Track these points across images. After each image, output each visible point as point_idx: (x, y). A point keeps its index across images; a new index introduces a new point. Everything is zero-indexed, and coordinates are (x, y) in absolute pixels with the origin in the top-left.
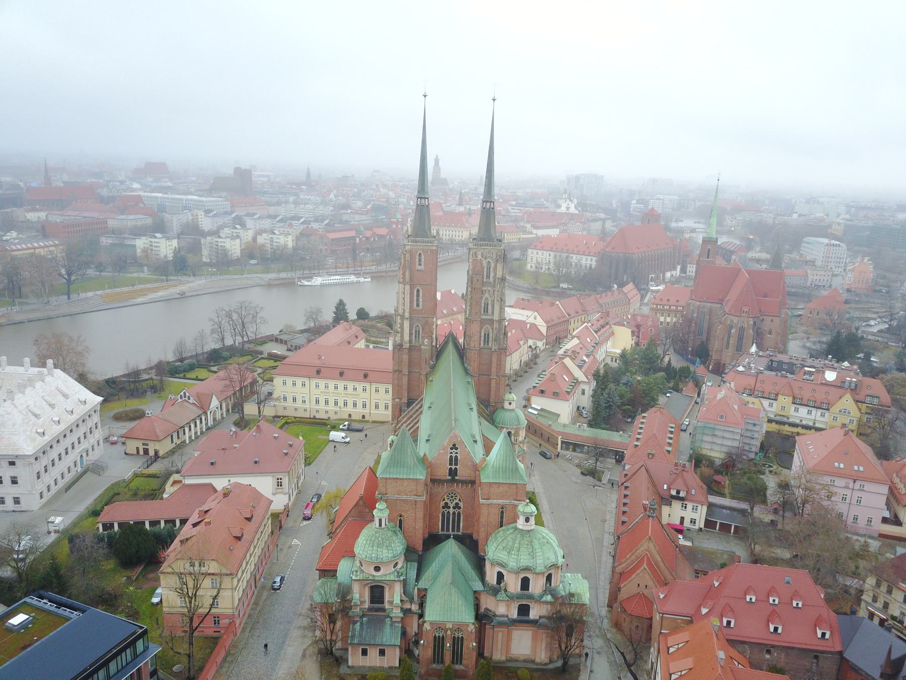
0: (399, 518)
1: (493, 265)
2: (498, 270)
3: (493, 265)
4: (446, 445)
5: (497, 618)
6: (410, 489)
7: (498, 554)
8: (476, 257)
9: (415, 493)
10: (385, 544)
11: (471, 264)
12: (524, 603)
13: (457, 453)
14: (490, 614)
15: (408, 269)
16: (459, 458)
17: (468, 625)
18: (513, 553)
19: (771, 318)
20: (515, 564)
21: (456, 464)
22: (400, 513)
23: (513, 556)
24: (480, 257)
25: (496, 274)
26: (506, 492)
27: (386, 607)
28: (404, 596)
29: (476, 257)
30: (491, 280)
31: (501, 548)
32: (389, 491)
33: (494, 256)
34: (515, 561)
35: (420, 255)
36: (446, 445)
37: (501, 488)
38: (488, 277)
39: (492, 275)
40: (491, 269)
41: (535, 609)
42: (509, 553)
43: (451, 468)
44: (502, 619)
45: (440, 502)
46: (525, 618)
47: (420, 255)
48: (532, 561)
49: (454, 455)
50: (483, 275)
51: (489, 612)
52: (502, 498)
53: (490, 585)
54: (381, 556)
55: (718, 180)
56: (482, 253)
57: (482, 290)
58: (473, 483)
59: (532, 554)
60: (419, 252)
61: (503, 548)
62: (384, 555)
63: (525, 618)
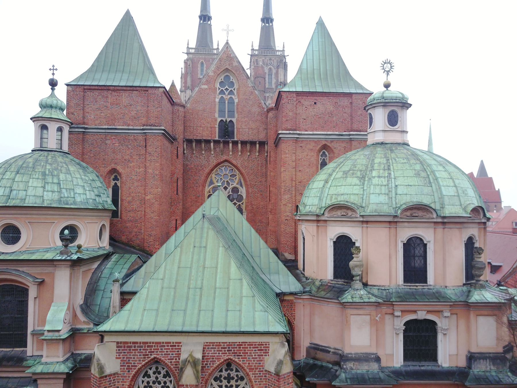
0: (113, 183)
1: (274, 71)
2: (279, 75)
3: (274, 71)
4: (211, 74)
5: (349, 365)
6: (133, 113)
7: (333, 191)
8: (257, 64)
9: (144, 121)
10: (39, 169)
11: (253, 71)
12: (421, 315)
13: (231, 92)
14: (325, 360)
15: (189, 74)
16: (236, 101)
17: (264, 349)
18: (374, 173)
19: (494, 204)
20: (383, 199)
22: (113, 166)
23: (375, 181)
24: (261, 63)
25: (277, 80)
26: (331, 114)
27: (29, 353)
28: (82, 317)
29: (257, 64)
30: (274, 86)
31: (340, 175)
32: (90, 116)
33: (275, 64)
34: (384, 190)
35: (202, 63)
36: (211, 74)
37: (319, 105)
38: (270, 83)
39: (274, 81)
40: (273, 76)
42: (362, 178)
44: (363, 369)
45: (204, 186)
46: (427, 366)
47: (202, 63)
48: (427, 190)
49: (226, 97)
50: (265, 78)
51: (320, 355)
52: (322, 128)
53: (318, 283)
54: (22, 194)
55: (430, 120)
56: (263, 60)
57: (265, 97)
58: (262, 144)
59: (423, 174)
60: (201, 61)
61: (345, 173)
62: (30, 192)
63: (427, 366)
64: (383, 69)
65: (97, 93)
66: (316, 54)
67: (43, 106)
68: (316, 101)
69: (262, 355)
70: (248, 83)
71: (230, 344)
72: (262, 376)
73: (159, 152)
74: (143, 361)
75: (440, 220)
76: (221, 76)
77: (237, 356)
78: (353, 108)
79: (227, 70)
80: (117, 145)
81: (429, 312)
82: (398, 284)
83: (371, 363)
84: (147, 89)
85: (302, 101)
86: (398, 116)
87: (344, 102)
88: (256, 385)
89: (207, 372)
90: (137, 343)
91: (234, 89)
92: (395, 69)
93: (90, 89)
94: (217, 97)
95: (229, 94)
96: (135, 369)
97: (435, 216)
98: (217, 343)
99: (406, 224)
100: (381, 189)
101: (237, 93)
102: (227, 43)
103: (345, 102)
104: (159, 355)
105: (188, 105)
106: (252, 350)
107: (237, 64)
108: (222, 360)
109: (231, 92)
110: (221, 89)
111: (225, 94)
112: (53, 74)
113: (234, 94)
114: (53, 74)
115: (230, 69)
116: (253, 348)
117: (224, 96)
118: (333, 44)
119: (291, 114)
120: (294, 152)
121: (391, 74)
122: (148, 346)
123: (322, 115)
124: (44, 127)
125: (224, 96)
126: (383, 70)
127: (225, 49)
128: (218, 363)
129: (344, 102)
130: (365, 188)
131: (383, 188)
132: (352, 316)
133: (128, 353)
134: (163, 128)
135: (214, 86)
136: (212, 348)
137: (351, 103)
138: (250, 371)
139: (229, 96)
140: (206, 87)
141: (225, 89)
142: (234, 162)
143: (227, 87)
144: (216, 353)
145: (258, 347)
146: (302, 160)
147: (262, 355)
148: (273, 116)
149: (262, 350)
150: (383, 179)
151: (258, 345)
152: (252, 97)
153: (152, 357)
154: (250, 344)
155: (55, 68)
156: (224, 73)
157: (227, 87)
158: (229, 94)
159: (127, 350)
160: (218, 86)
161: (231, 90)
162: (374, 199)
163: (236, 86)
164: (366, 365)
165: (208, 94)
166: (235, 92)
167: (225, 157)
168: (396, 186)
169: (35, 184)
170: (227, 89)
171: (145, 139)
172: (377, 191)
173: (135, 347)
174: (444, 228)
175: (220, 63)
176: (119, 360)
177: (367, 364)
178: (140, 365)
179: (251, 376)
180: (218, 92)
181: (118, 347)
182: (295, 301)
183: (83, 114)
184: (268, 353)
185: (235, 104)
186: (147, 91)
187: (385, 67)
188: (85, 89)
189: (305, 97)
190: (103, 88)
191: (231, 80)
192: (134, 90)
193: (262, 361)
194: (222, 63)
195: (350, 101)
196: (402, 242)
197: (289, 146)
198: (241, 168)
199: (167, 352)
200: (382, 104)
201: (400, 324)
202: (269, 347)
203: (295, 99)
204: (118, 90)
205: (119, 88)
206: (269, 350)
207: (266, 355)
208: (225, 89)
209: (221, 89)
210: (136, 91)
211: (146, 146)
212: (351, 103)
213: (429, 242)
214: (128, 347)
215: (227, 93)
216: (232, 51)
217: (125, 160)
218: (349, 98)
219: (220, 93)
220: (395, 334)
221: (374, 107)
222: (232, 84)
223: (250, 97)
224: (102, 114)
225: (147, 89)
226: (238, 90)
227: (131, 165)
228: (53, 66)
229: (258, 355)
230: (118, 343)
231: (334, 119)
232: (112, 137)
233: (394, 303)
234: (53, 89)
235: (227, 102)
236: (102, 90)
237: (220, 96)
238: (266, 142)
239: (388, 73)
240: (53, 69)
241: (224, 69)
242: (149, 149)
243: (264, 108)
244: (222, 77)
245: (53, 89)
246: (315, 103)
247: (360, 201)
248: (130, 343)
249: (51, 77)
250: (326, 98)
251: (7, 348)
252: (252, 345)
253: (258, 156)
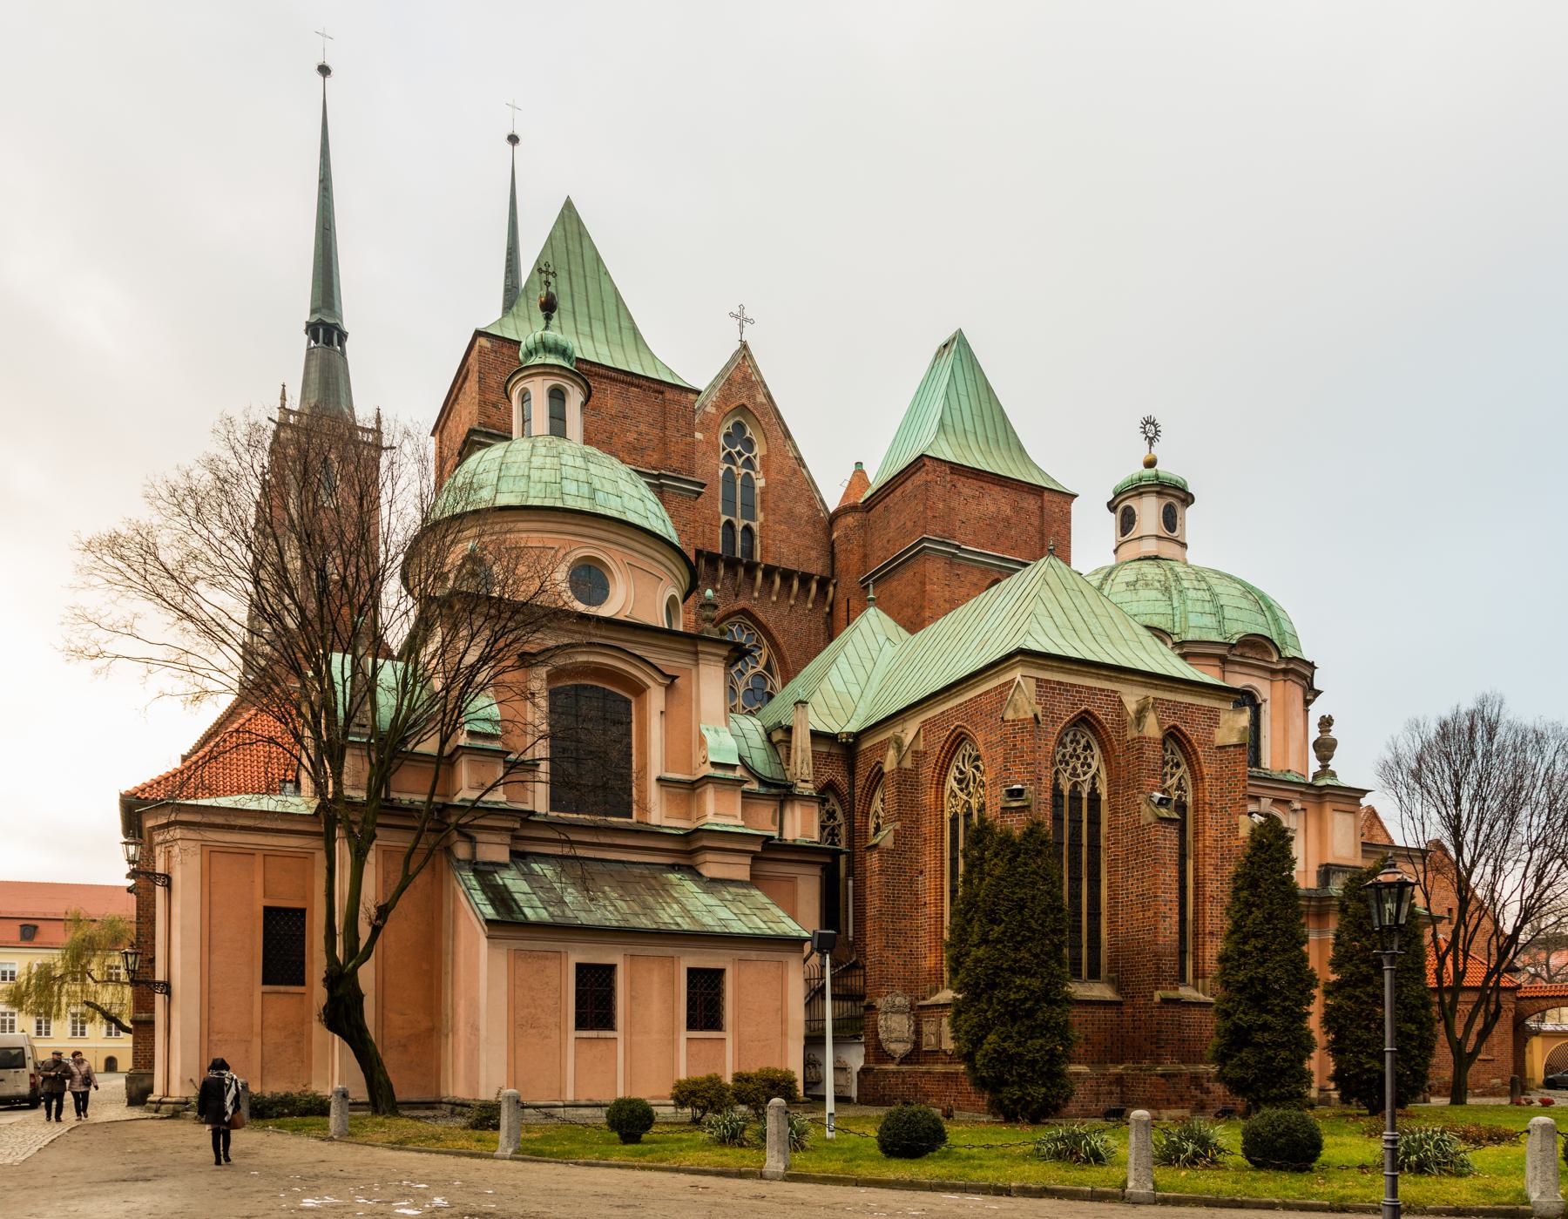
21: (749, 512)
43: (729, 524)
70: (787, 448)
73: (692, 535)
74: (1072, 712)
85: (959, 485)
91: (755, 457)
95: (744, 466)
97: (1275, 658)
100: (1204, 607)
101: (762, 466)
103: (1031, 503)
109: (749, 463)
110: (729, 449)
111: (735, 464)
115: (749, 406)
117: (734, 468)
119: (941, 506)
125: (734, 468)
130: (1175, 605)
131: (1206, 604)
142: (761, 616)
143: (739, 448)
148: (856, 524)
150: (1201, 592)
152: (795, 481)
153: (1083, 707)
156: (734, 416)
160: (722, 441)
162: (1194, 620)
165: (704, 454)
166: (757, 463)
167: (742, 603)
170: (740, 454)
173: (1060, 689)
180: (722, 455)
181: (1038, 686)
185: (757, 491)
191: (748, 435)
194: (733, 389)
198: (775, 633)
209: (729, 449)
215: (740, 462)
222: (749, 444)
223: (791, 481)
230: (1037, 679)
237: (726, 466)
239: (1151, 441)
241: (737, 404)
244: (730, 423)
247: (1170, 624)
253: (810, 610)
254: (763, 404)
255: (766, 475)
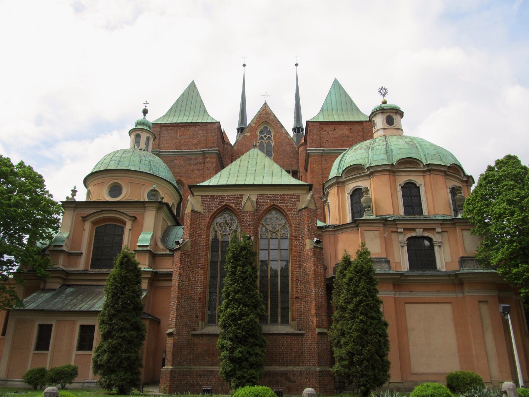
6: (195, 141)
16: (273, 144)
17: (297, 198)
37: (337, 130)
41: (446, 247)
64: (380, 93)
65: (169, 129)
66: (334, 100)
67: (138, 124)
68: (335, 128)
69: (296, 202)
70: (282, 130)
71: (274, 195)
72: (296, 215)
74: (218, 206)
75: (426, 169)
76: (260, 127)
77: (279, 202)
78: (365, 131)
79: (266, 122)
80: (183, 163)
81: (425, 230)
82: (400, 215)
83: (382, 264)
84: (206, 124)
86: (393, 119)
87: (357, 128)
88: (292, 220)
89: (260, 213)
90: (214, 196)
91: (271, 136)
92: (389, 93)
93: (165, 126)
94: (258, 141)
95: (267, 140)
96: (212, 211)
98: (266, 195)
99: (402, 174)
102: (265, 103)
104: (228, 202)
105: (235, 148)
106: (289, 199)
107: (273, 118)
108: (270, 205)
111: (264, 139)
112: (146, 106)
113: (271, 139)
114: (146, 106)
115: (267, 121)
116: (290, 197)
117: (263, 141)
118: (345, 93)
120: (320, 163)
121: (386, 96)
122: (221, 198)
123: (340, 138)
124: (138, 136)
125: (263, 141)
126: (381, 94)
127: (264, 108)
128: (267, 207)
129: (357, 128)
132: (365, 232)
133: (208, 202)
134: (218, 149)
135: (255, 133)
136: (262, 198)
137: (363, 128)
138: (288, 212)
139: (267, 141)
140: (249, 134)
141: (264, 136)
143: (265, 134)
144: (265, 201)
145: (293, 197)
146: (327, 169)
147: (296, 202)
149: (296, 199)
151: (293, 196)
153: (224, 204)
154: (288, 195)
155: (147, 103)
156: (263, 125)
157: (265, 134)
158: (267, 140)
159: (208, 200)
160: (258, 134)
161: (269, 137)
163: (273, 134)
164: (379, 265)
166: (272, 138)
168: (392, 150)
169: (134, 159)
170: (265, 136)
171: (204, 158)
172: (378, 153)
174: (430, 174)
175: (260, 118)
176: (203, 207)
177: (379, 264)
178: (216, 209)
179: (289, 214)
180: (258, 138)
181: (202, 199)
182: (322, 235)
183: (159, 143)
184: (300, 200)
185: (272, 146)
186: (207, 126)
187: (381, 92)
188: (161, 126)
189: (326, 126)
190: (174, 125)
192: (197, 126)
193: (296, 205)
195: (362, 127)
196: (400, 185)
197: (316, 159)
199: (233, 201)
200: (381, 111)
201: (404, 238)
202: (300, 197)
203: (319, 127)
204: (185, 126)
205: (186, 125)
206: (300, 199)
207: (298, 202)
208: (264, 136)
210: (199, 126)
211: (204, 163)
212: (363, 128)
213: (421, 185)
214: (208, 198)
215: (265, 139)
216: (269, 109)
217: (188, 174)
218: (361, 125)
219: (260, 139)
220: (400, 247)
221: (376, 115)
222: (270, 132)
223: (284, 140)
224: (173, 143)
225: (206, 124)
226: (274, 136)
227: (192, 177)
228: (146, 102)
229: (293, 202)
230: (202, 196)
231: (350, 139)
232: (179, 158)
233: (397, 222)
234: (145, 115)
235: (265, 145)
236: (173, 126)
237: (260, 141)
238: (298, 171)
240: (146, 103)
241: (263, 121)
242: (206, 164)
243: (295, 148)
244: (262, 128)
245: (145, 115)
246: (335, 129)
248: (210, 196)
249: (145, 108)
250: (343, 125)
251: (105, 269)
252: (289, 196)
254: (272, 119)
255: (275, 141)
